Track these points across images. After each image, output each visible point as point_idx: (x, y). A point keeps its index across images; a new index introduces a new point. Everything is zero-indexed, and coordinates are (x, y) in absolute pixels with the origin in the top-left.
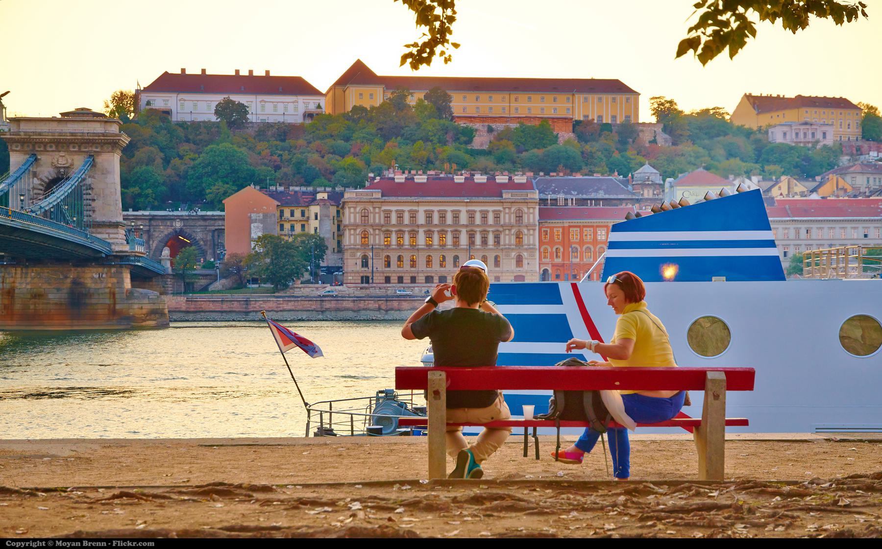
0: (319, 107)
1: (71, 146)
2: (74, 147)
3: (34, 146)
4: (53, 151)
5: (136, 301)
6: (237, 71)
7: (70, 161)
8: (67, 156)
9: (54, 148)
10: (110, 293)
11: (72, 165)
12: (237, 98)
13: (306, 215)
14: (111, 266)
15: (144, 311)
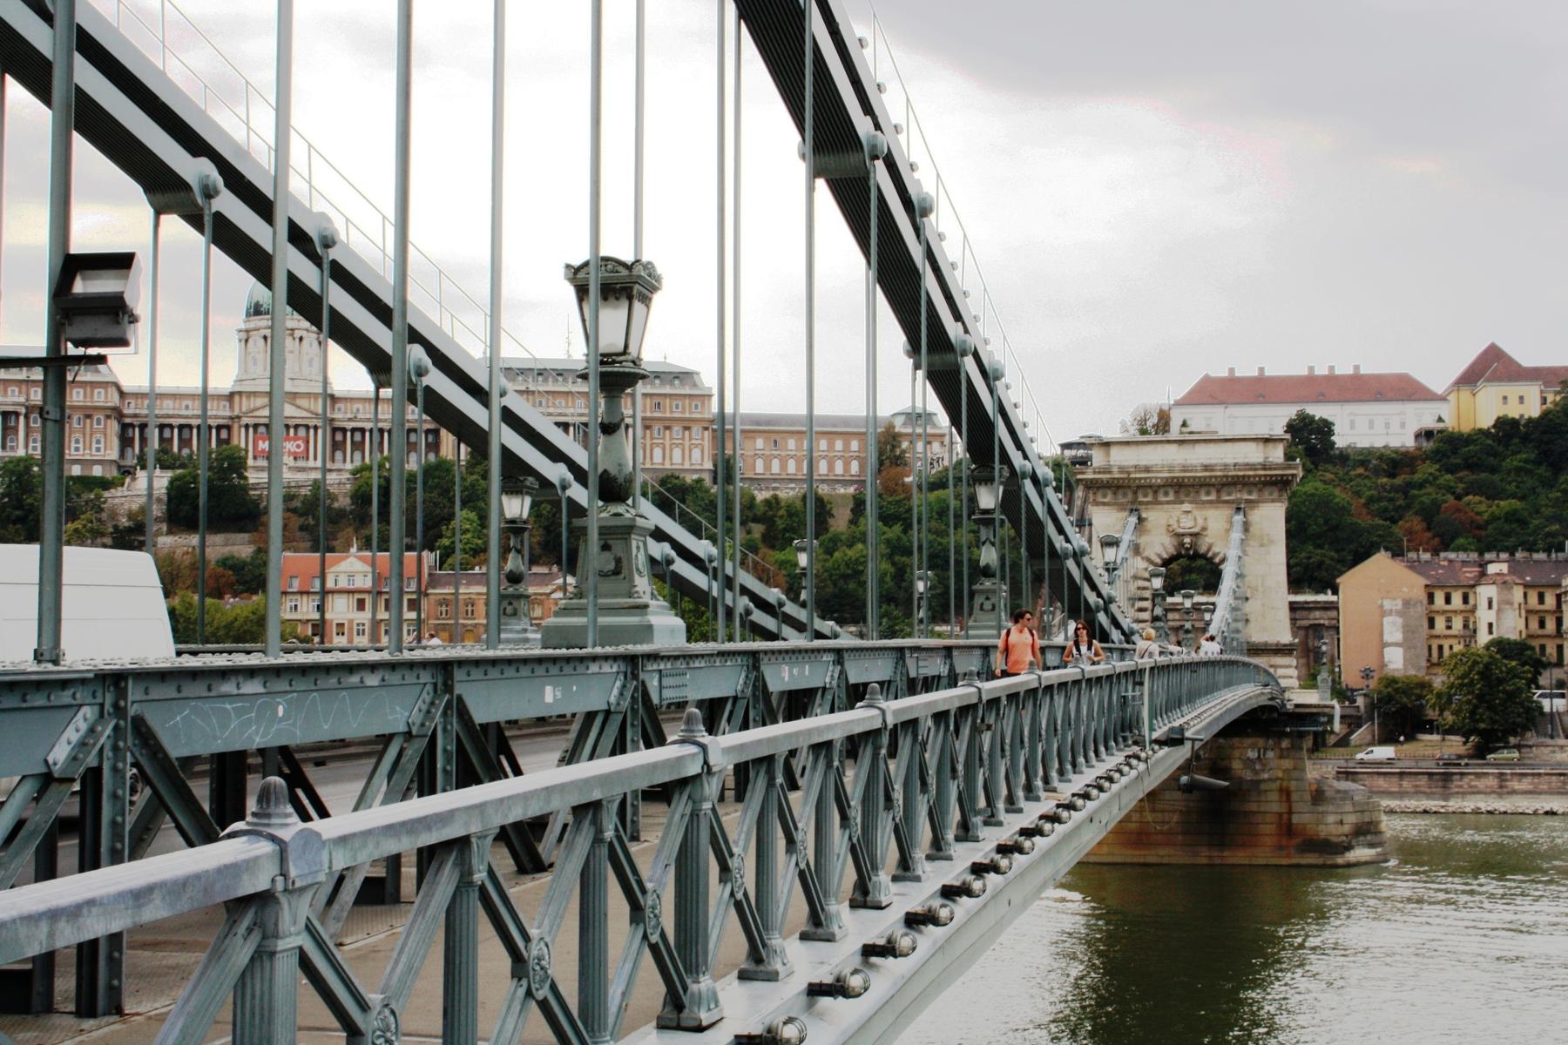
0: (1440, 420)
1: (1203, 491)
2: (1208, 493)
3: (1135, 493)
4: (1168, 503)
5: (1331, 808)
6: (1311, 369)
7: (1200, 522)
8: (1196, 512)
9: (1171, 497)
10: (1281, 790)
11: (1204, 529)
12: (1318, 411)
13: (1471, 601)
14: (1282, 735)
15: (1347, 828)
